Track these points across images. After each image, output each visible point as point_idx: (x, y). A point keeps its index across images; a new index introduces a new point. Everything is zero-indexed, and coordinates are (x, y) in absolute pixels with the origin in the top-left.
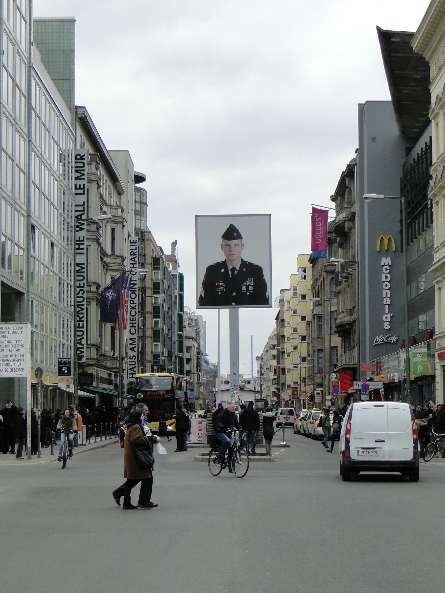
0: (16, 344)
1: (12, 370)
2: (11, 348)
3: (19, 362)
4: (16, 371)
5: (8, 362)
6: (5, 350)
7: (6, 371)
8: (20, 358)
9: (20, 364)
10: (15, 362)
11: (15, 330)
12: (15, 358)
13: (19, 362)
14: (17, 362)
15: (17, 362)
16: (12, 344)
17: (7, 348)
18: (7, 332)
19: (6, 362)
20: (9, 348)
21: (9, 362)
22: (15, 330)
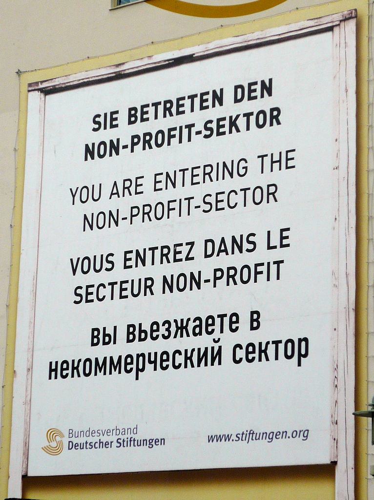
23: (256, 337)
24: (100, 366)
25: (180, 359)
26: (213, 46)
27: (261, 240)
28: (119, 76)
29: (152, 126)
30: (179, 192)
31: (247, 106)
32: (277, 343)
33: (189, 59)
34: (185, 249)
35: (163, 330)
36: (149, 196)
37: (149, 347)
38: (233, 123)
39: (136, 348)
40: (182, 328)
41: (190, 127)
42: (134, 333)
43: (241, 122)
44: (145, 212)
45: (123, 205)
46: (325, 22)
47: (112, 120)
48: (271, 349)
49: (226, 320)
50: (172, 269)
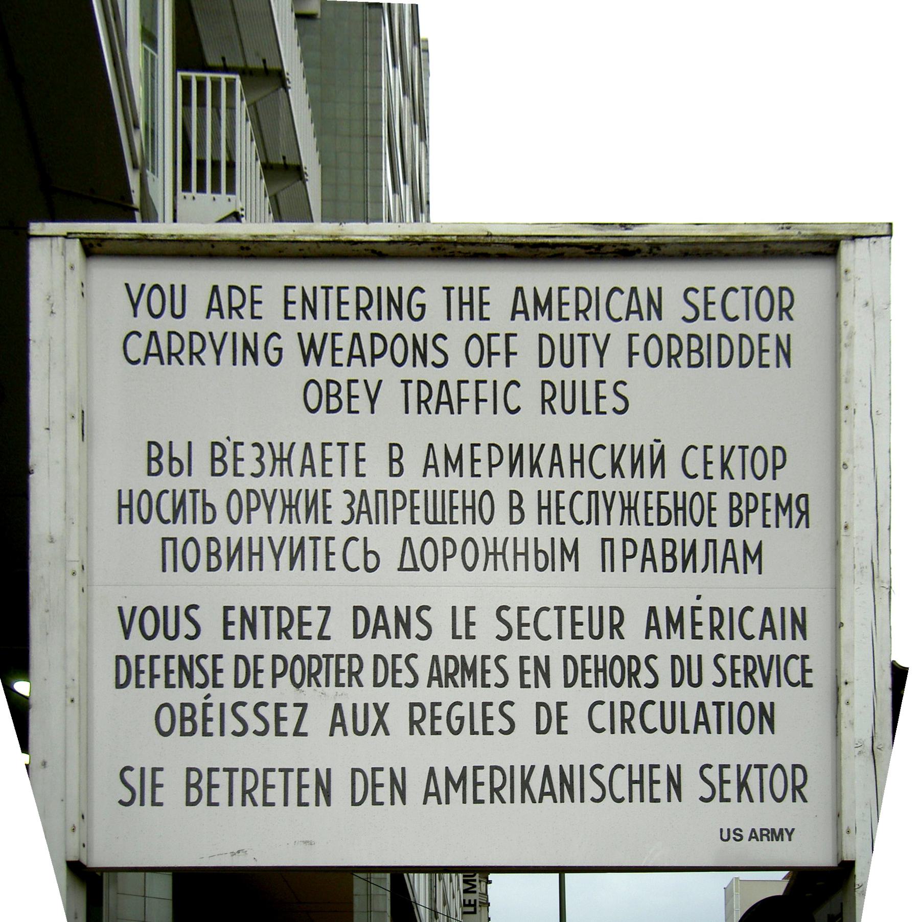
0: (722, 488)
1: (675, 784)
2: (657, 534)
3: (757, 695)
4: (716, 793)
5: (625, 693)
6: (590, 553)
7: (607, 790)
8: (766, 648)
9: (767, 716)
10: (708, 693)
11: (701, 327)
12: (708, 648)
13: (757, 695)
14: (727, 694)
15: (727, 694)
16: (674, 481)
17: (618, 532)
18: (617, 350)
19: (610, 694)
20: (639, 533)
21: (637, 696)
22: (701, 327)
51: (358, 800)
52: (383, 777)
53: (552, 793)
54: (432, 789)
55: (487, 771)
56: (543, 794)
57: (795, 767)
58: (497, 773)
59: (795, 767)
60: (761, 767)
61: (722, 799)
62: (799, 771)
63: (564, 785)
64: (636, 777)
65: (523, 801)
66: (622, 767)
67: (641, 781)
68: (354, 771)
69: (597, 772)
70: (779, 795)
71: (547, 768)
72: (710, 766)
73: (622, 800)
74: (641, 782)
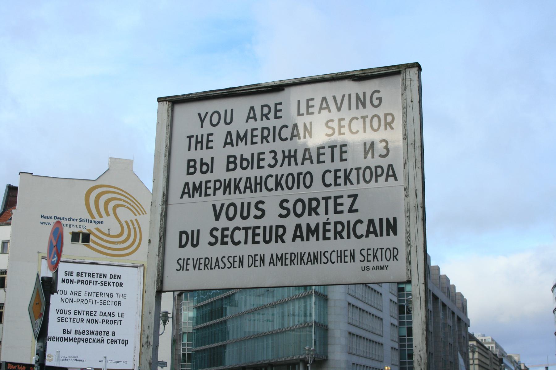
1: (352, 256)
4: (366, 259)
7: (329, 260)
23: (114, 338)
24: (66, 339)
25: (91, 341)
26: (104, 262)
27: (116, 315)
28: (74, 262)
29: (85, 278)
30: (92, 298)
31: (113, 280)
32: (120, 340)
33: (97, 264)
34: (94, 313)
35: (86, 333)
36: (82, 297)
37: (81, 336)
38: (109, 284)
39: (78, 336)
40: (92, 333)
41: (96, 282)
42: (76, 332)
43: (112, 284)
44: (82, 301)
45: (75, 298)
46: (136, 265)
47: (71, 274)
48: (118, 341)
49: (105, 333)
50: (90, 317)
51: (250, 265)
52: (258, 258)
53: (311, 261)
54: (272, 261)
55: (289, 254)
56: (308, 261)
57: (394, 248)
58: (293, 255)
59: (394, 248)
60: (382, 249)
61: (368, 261)
62: (395, 250)
63: (315, 258)
64: (339, 255)
65: (301, 264)
66: (334, 251)
67: (341, 256)
68: (249, 256)
69: (326, 254)
70: (388, 259)
71: (309, 253)
72: (364, 249)
73: (334, 262)
74: (341, 256)
